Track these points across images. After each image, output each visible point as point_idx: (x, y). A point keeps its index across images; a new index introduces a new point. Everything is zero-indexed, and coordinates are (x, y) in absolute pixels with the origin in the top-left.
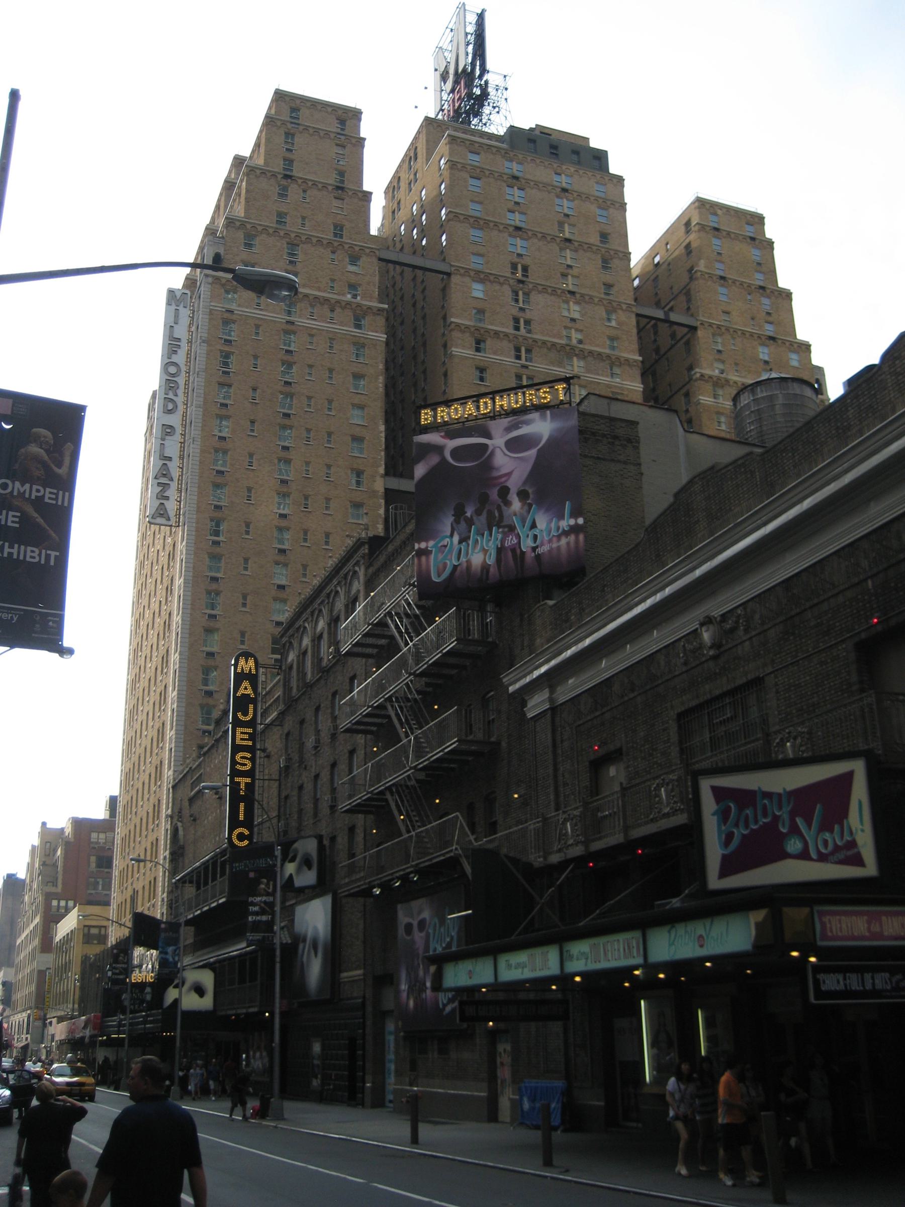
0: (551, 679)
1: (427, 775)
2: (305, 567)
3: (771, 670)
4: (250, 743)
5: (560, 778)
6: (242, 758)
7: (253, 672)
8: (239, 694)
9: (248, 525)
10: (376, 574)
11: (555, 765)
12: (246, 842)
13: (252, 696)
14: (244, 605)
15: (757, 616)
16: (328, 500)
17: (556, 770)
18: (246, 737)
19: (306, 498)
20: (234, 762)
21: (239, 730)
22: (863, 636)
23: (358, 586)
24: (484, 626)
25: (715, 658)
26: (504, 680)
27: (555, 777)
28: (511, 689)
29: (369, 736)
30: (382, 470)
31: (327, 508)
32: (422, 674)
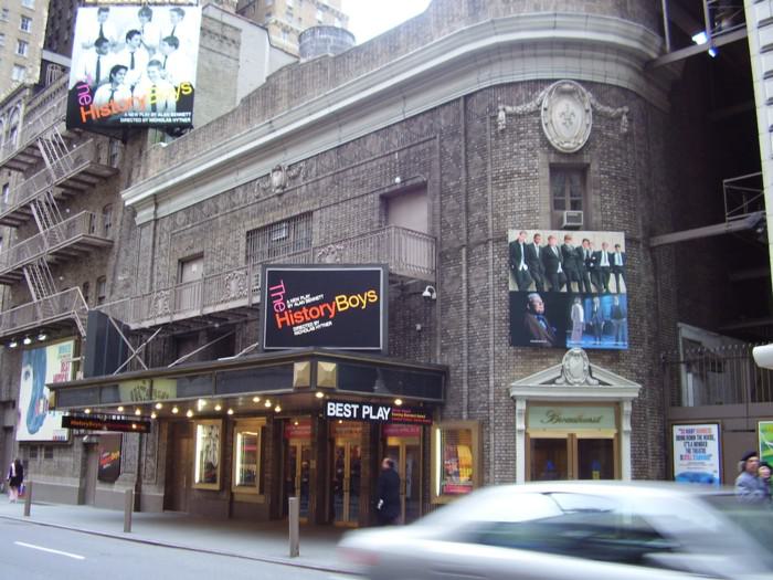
0: (156, 199)
1: (57, 259)
3: (318, 206)
5: (155, 269)
10: (33, 111)
11: (153, 260)
15: (314, 169)
17: (153, 263)
22: (387, 190)
23: (18, 118)
24: (112, 158)
25: (280, 195)
26: (123, 196)
27: (152, 268)
28: (127, 203)
30: (41, 45)
32: (61, 186)
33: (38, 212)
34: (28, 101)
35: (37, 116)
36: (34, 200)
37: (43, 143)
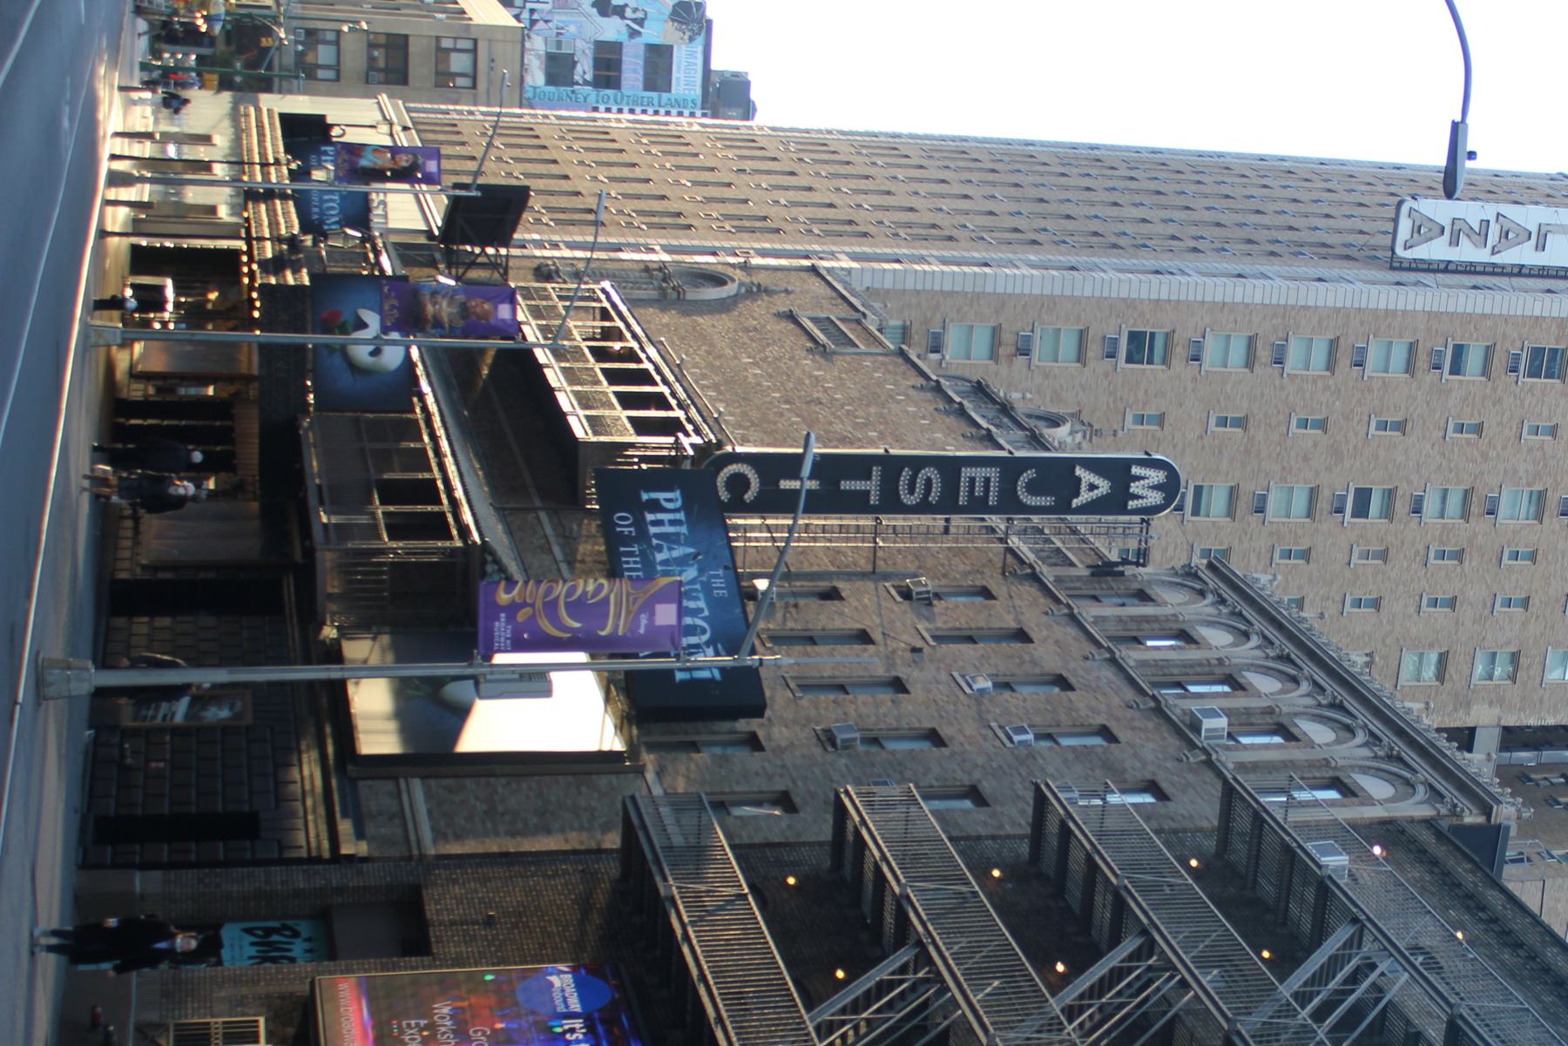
2: (1306, 555)
4: (962, 500)
6: (929, 482)
7: (1132, 504)
8: (1079, 471)
9: (1401, 426)
10: (1421, 855)
12: (724, 495)
13: (1076, 502)
14: (1223, 422)
16: (1452, 603)
18: (978, 491)
19: (1459, 556)
20: (917, 463)
21: (993, 473)
23: (1381, 796)
29: (1024, 849)
30: (1511, 721)
31: (1434, 603)
33: (1117, 974)
34: (1444, 824)
35: (1417, 872)
36: (1152, 943)
37: (1348, 944)
